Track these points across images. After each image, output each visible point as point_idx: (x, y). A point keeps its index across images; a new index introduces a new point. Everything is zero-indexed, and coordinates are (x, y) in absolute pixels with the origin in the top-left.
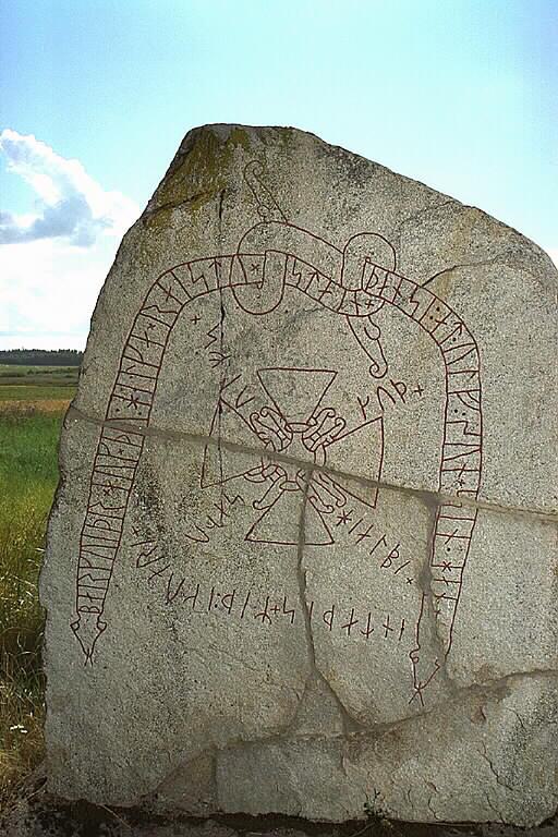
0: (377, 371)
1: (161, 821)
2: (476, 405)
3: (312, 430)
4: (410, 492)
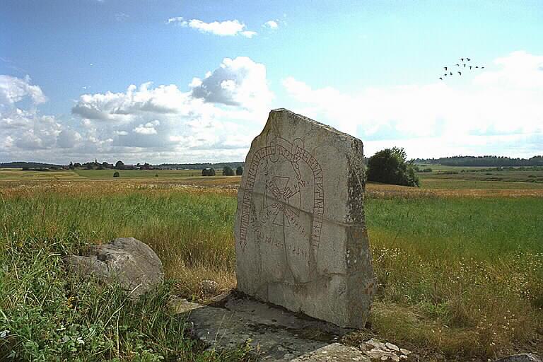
0: (298, 177)
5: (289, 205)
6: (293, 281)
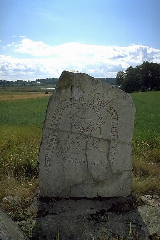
1: (61, 199)
2: (117, 124)
3: (88, 129)
4: (106, 140)
5: (91, 136)
6: (93, 181)
